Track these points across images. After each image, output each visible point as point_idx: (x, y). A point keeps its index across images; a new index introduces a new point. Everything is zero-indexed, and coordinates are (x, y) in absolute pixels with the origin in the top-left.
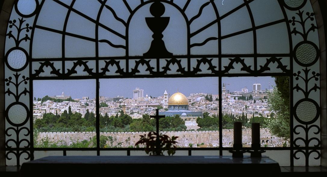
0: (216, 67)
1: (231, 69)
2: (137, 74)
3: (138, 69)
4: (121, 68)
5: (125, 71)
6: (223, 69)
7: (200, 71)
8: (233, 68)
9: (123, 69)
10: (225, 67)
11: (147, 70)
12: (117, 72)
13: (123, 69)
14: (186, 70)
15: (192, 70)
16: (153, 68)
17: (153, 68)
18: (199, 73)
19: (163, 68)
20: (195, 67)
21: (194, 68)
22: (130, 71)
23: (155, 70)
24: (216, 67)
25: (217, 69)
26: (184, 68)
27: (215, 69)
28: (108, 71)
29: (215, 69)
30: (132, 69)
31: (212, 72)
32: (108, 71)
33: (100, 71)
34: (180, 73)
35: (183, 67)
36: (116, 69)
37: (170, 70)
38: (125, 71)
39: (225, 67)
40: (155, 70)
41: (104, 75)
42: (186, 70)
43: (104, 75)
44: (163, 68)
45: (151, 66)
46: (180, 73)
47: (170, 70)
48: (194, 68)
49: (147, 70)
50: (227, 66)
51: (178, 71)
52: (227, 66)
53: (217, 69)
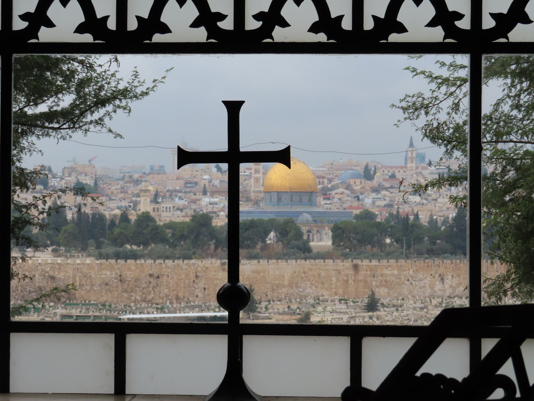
0: (460, 16)
1: (519, 26)
2: (157, 38)
3: (164, 18)
4: (99, 15)
5: (112, 25)
6: (488, 23)
7: (401, 29)
8: (526, 20)
9: (106, 18)
10: (493, 16)
11: (195, 24)
12: (80, 29)
13: (106, 18)
14: (347, 25)
15: (369, 25)
16: (222, 17)
17: (222, 17)
18: (394, 38)
19: (257, 17)
20: (382, 15)
21: (374, 17)
22: (132, 25)
23: (227, 25)
24: (460, 16)
25: (464, 24)
26: (340, 18)
27: (458, 24)
28: (50, 24)
29: (458, 24)
30: (139, 18)
31: (445, 38)
32: (50, 24)
33: (19, 25)
34: (322, 37)
35: (333, 16)
36: (82, 19)
37: (284, 24)
38: (112, 25)
39: (493, 16)
40: (227, 25)
41: (34, 41)
42: (347, 25)
43: (34, 41)
44: (257, 17)
45: (213, 10)
46: (322, 37)
47: (284, 24)
48: (374, 17)
49: (195, 25)
50: (505, 11)
51: (314, 28)
52: (505, 11)
53: (464, 24)
